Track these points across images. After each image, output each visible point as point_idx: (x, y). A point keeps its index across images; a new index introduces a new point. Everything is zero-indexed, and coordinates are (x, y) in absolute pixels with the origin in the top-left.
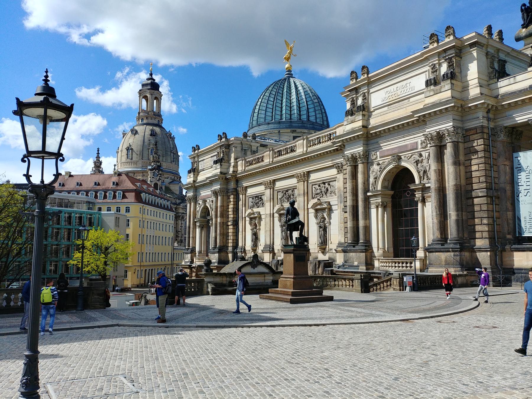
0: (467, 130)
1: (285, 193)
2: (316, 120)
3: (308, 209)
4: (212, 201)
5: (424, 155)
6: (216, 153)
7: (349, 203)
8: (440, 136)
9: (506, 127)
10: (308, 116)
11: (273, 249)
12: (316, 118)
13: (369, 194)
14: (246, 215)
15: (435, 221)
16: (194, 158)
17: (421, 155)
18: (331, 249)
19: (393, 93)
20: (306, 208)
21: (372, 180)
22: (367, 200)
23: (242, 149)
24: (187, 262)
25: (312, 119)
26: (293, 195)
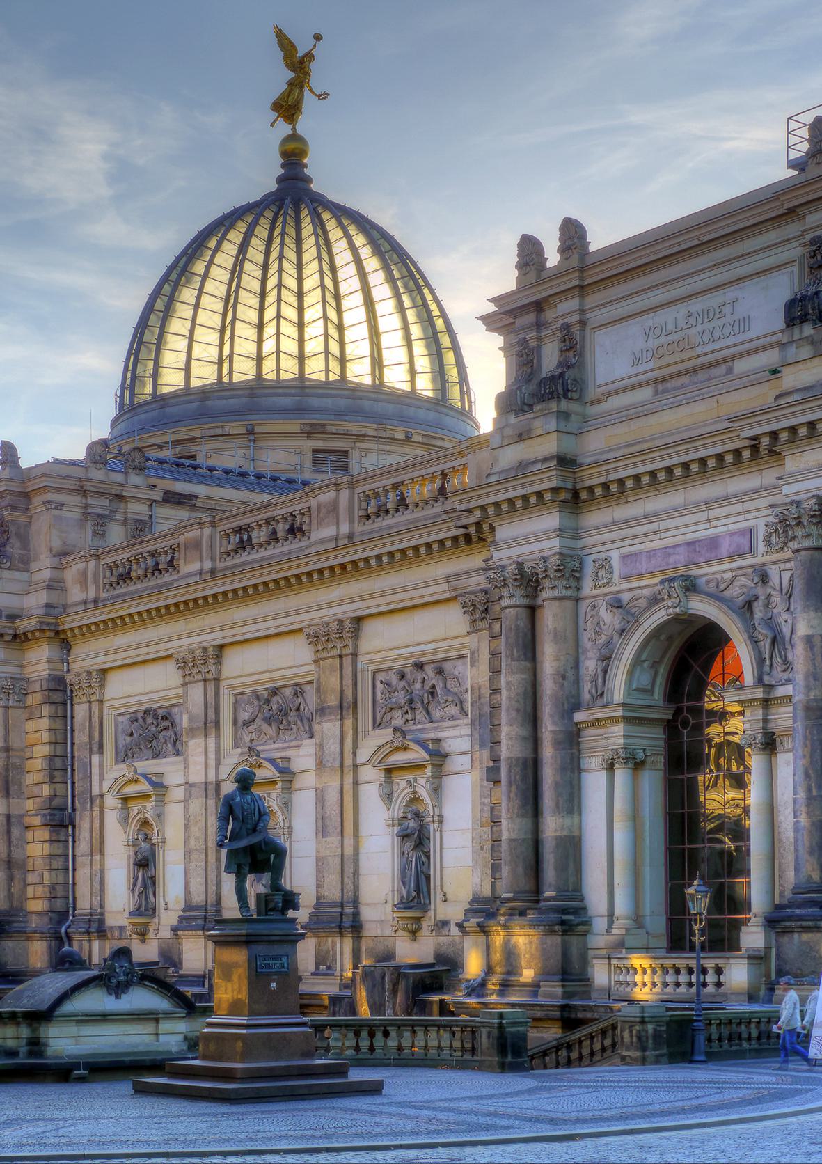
1: (268, 702)
2: (413, 380)
3: (356, 767)
5: (774, 579)
10: (377, 364)
12: (413, 373)
14: (106, 785)
15: (804, 821)
17: (764, 578)
19: (675, 337)
20: (348, 762)
21: (590, 665)
26: (298, 709)
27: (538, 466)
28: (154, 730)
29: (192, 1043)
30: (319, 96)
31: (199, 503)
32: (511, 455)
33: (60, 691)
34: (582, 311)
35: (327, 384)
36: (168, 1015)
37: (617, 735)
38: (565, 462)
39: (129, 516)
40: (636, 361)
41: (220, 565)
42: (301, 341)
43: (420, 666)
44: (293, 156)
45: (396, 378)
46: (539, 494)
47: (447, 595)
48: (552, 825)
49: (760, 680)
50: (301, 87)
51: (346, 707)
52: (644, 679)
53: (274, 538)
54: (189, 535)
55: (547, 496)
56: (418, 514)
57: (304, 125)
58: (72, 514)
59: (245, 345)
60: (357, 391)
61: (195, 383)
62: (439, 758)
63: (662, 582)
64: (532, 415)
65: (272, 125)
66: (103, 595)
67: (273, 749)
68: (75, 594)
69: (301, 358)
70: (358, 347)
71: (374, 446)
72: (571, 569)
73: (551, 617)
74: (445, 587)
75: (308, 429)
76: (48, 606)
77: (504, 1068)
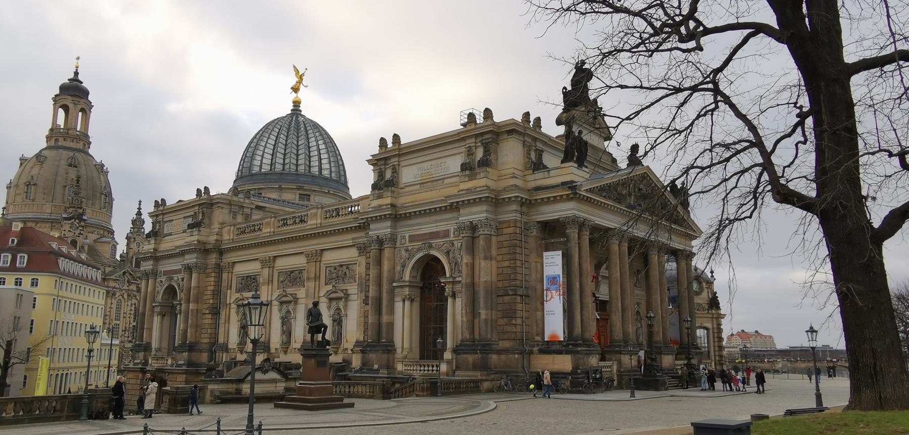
0: (500, 223)
4: (183, 279)
6: (192, 213)
7: (372, 293)
8: (473, 227)
9: (539, 222)
10: (320, 169)
11: (269, 347)
12: (331, 172)
13: (394, 284)
16: (157, 216)
18: (347, 349)
21: (398, 268)
22: (392, 291)
24: (138, 364)
25: (326, 173)
28: (250, 283)
29: (287, 389)
32: (376, 203)
33: (219, 269)
36: (280, 381)
37: (406, 291)
38: (393, 206)
42: (297, 160)
43: (341, 266)
48: (385, 318)
49: (451, 276)
51: (317, 278)
52: (414, 274)
53: (295, 223)
56: (343, 218)
59: (279, 159)
62: (347, 296)
67: (290, 290)
68: (226, 237)
69: (297, 165)
70: (315, 162)
72: (393, 239)
73: (387, 253)
77: (384, 398)
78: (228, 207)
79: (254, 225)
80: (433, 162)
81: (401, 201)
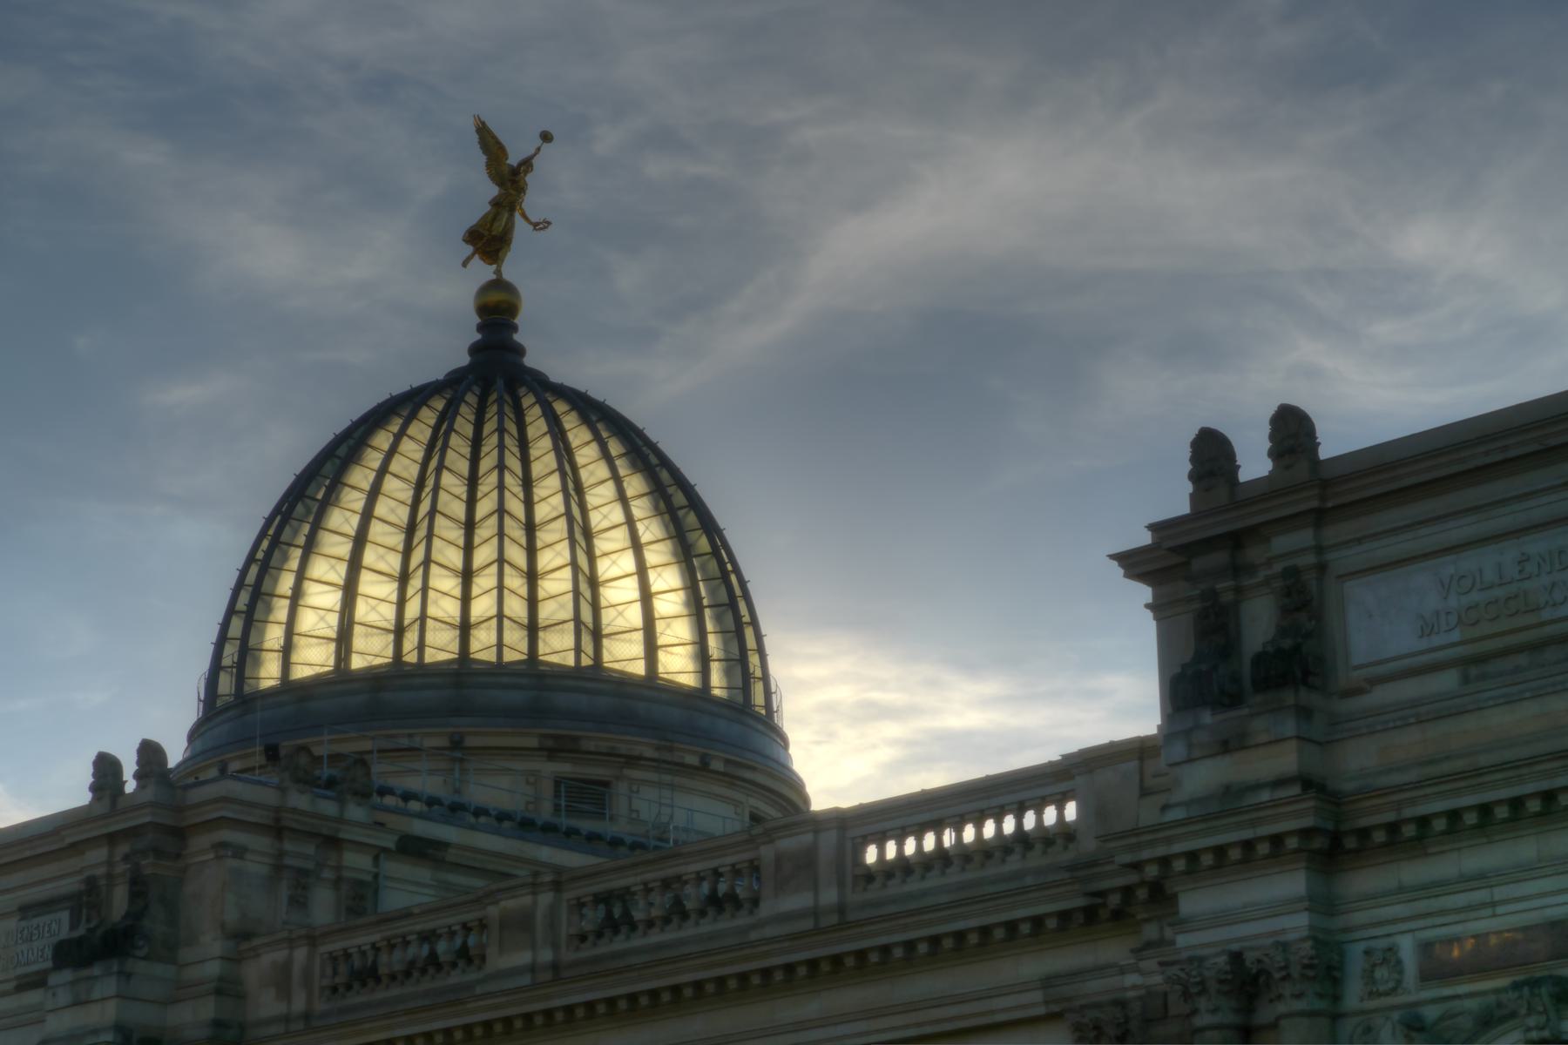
6: (70, 885)
19: (1499, 593)
23: (278, 869)
27: (1265, 796)
30: (535, 225)
31: (451, 855)
32: (1204, 777)
34: (1319, 549)
35: (577, 672)
39: (347, 874)
40: (1427, 629)
41: (568, 956)
42: (533, 602)
44: (497, 314)
45: (677, 665)
46: (1277, 840)
47: (1041, 1011)
50: (512, 210)
54: (509, 904)
55: (1292, 843)
57: (513, 268)
58: (256, 867)
60: (622, 683)
61: (357, 663)
63: (1516, 986)
64: (1246, 711)
65: (465, 264)
66: (320, 1006)
68: (266, 1005)
71: (652, 776)
72: (1325, 968)
74: (1037, 996)
75: (550, 743)
76: (218, 1024)
78: (260, 843)
79: (428, 937)
80: (1535, 545)
81: (1358, 760)
